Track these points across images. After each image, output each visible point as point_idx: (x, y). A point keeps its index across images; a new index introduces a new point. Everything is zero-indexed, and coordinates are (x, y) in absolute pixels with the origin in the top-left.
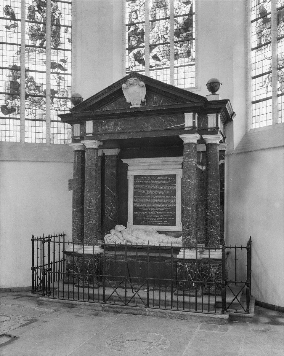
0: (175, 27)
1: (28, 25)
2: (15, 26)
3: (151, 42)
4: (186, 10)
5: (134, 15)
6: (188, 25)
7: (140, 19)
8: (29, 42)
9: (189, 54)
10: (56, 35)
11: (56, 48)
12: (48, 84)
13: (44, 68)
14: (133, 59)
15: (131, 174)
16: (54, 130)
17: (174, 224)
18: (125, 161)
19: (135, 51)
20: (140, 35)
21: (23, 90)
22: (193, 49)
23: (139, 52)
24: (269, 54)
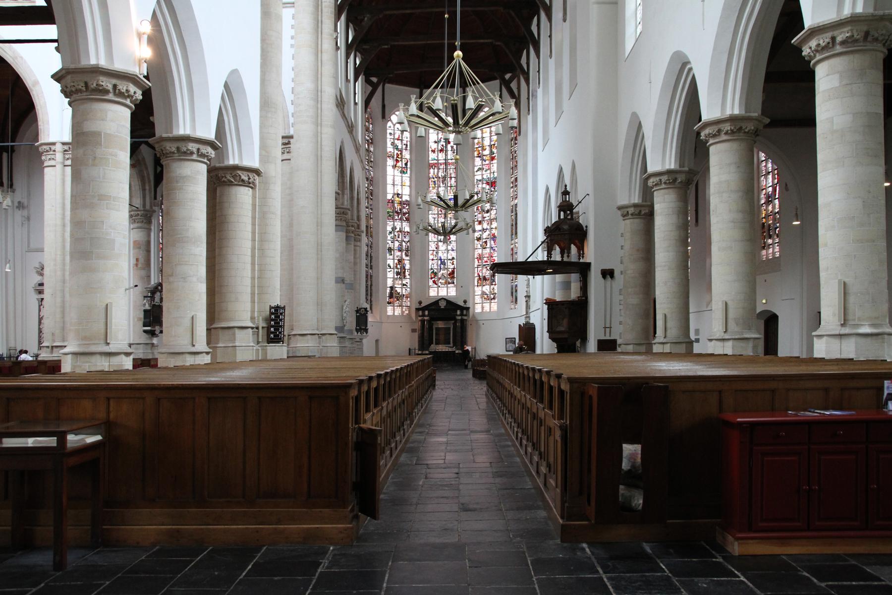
0: (449, 272)
1: (396, 270)
2: (391, 271)
3: (439, 276)
4: (452, 267)
5: (432, 265)
6: (453, 272)
7: (435, 268)
8: (396, 277)
9: (453, 283)
10: (404, 272)
11: (404, 278)
12: (402, 292)
13: (400, 286)
14: (432, 282)
15: (434, 327)
16: (404, 310)
17: (449, 344)
18: (433, 322)
19: (433, 279)
20: (435, 274)
21: (394, 295)
22: (455, 281)
23: (435, 280)
24: (481, 289)
